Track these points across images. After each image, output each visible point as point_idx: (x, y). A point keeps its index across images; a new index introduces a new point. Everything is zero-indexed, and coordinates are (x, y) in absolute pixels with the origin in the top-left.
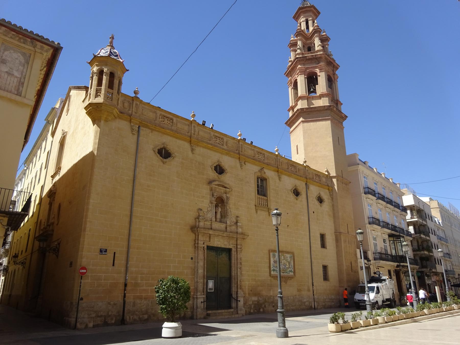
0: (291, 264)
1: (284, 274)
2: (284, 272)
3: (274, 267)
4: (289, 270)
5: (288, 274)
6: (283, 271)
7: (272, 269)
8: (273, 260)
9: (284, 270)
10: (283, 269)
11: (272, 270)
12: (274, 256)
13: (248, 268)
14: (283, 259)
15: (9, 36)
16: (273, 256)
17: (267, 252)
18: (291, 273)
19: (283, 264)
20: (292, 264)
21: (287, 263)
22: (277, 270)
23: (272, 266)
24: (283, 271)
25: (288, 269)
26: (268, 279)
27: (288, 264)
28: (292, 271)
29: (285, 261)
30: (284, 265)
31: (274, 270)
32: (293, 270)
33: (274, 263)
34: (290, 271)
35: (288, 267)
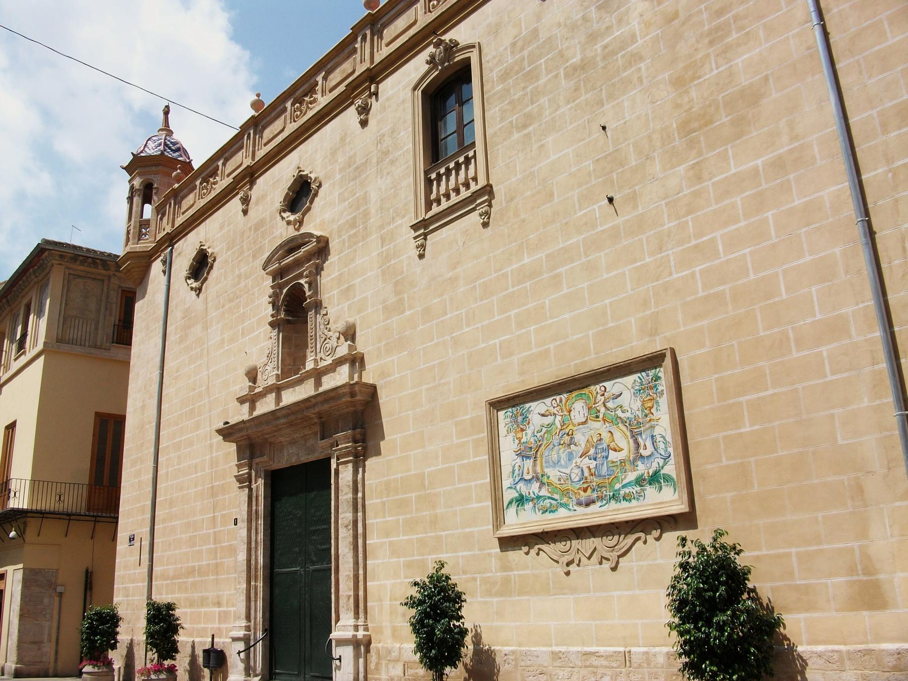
0: (652, 427)
1: (593, 508)
2: (595, 495)
3: (521, 486)
4: (631, 476)
5: (625, 504)
6: (585, 490)
7: (509, 495)
8: (515, 446)
9: (596, 481)
10: (583, 478)
11: (510, 503)
12: (520, 419)
13: (390, 519)
14: (584, 420)
15: (66, 260)
16: (516, 422)
17: (482, 412)
18: (650, 490)
19: (580, 450)
20: (657, 431)
21: (618, 435)
22: (539, 497)
23: (507, 482)
24: (585, 490)
25: (628, 467)
26: (490, 555)
27: (622, 440)
28: (667, 478)
29: (597, 425)
30: (592, 451)
31: (521, 500)
32: (670, 469)
33: (519, 460)
34: (640, 481)
35: (622, 462)
